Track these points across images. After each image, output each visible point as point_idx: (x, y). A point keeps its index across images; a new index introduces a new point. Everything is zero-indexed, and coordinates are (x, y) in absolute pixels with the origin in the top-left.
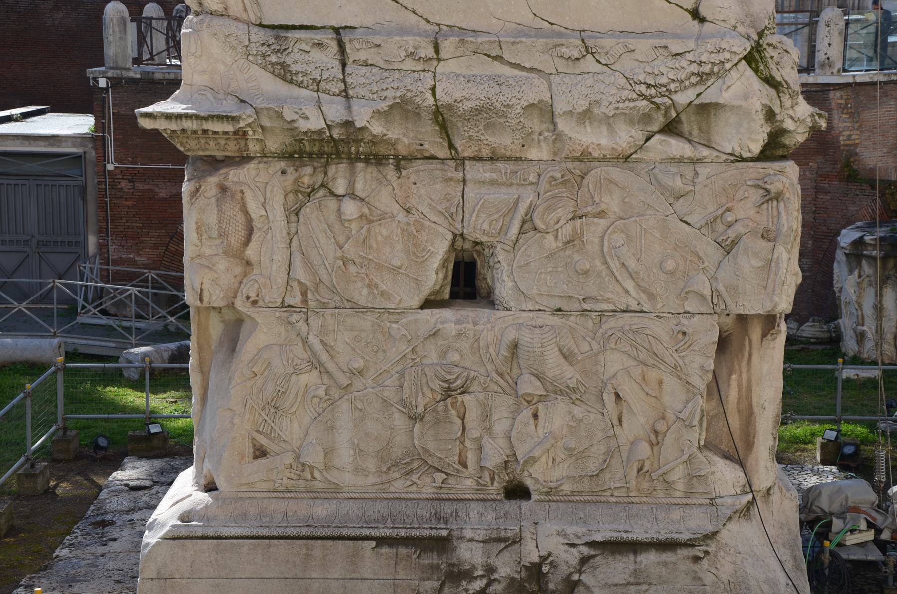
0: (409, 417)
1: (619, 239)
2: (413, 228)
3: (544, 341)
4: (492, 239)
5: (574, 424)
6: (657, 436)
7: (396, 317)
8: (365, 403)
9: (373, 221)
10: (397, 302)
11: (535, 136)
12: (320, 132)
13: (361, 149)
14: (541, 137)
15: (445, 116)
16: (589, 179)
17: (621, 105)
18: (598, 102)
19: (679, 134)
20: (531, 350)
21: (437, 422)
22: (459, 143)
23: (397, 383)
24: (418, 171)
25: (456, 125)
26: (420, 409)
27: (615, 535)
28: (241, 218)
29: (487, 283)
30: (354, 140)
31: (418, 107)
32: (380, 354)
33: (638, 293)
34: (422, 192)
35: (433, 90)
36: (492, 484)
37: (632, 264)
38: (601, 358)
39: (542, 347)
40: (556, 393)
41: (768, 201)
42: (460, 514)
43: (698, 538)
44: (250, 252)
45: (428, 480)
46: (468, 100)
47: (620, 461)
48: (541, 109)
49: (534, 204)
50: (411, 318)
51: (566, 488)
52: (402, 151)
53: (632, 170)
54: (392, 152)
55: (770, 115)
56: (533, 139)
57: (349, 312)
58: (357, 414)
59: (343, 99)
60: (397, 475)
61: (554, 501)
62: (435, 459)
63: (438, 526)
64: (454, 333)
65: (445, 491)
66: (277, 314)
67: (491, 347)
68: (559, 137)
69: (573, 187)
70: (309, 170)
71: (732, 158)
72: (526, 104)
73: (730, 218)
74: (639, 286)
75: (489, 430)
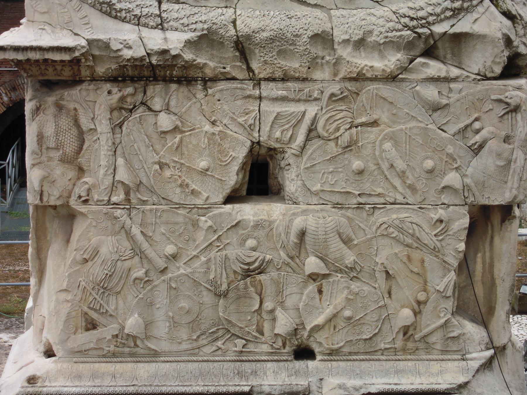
0: (215, 294)
1: (387, 145)
2: (217, 137)
3: (328, 229)
4: (283, 146)
5: (352, 297)
6: (419, 306)
7: (203, 211)
8: (179, 284)
9: (184, 132)
10: (204, 198)
11: (319, 61)
12: (142, 59)
13: (174, 73)
14: (324, 61)
15: (244, 44)
16: (363, 97)
17: (389, 34)
18: (371, 32)
19: (435, 57)
20: (316, 237)
21: (239, 298)
22: (255, 65)
23: (205, 266)
24: (222, 90)
25: (254, 52)
26: (224, 287)
27: (387, 387)
28: (74, 131)
29: (278, 182)
30: (169, 66)
31: (222, 37)
32: (191, 242)
33: (404, 189)
34: (225, 107)
35: (234, 22)
36: (284, 348)
37: (400, 165)
38: (374, 242)
39: (326, 234)
40: (337, 272)
41: (507, 113)
42: (258, 373)
43: (454, 388)
44: (81, 160)
45: (230, 345)
46: (263, 31)
47: (389, 327)
48: (323, 38)
49: (318, 116)
50: (216, 212)
51: (346, 350)
52: (209, 73)
53: (396, 87)
54: (200, 75)
55: (508, 42)
56: (317, 63)
57: (165, 207)
58: (173, 292)
59: (160, 31)
60: (205, 342)
61: (335, 361)
62: (237, 329)
63: (241, 383)
64: (252, 224)
65: (245, 354)
66: (105, 211)
67: (283, 235)
68: (338, 61)
69: (350, 102)
70: (130, 90)
71: (479, 77)
72: (311, 34)
73: (477, 125)
74: (405, 183)
75: (282, 304)
